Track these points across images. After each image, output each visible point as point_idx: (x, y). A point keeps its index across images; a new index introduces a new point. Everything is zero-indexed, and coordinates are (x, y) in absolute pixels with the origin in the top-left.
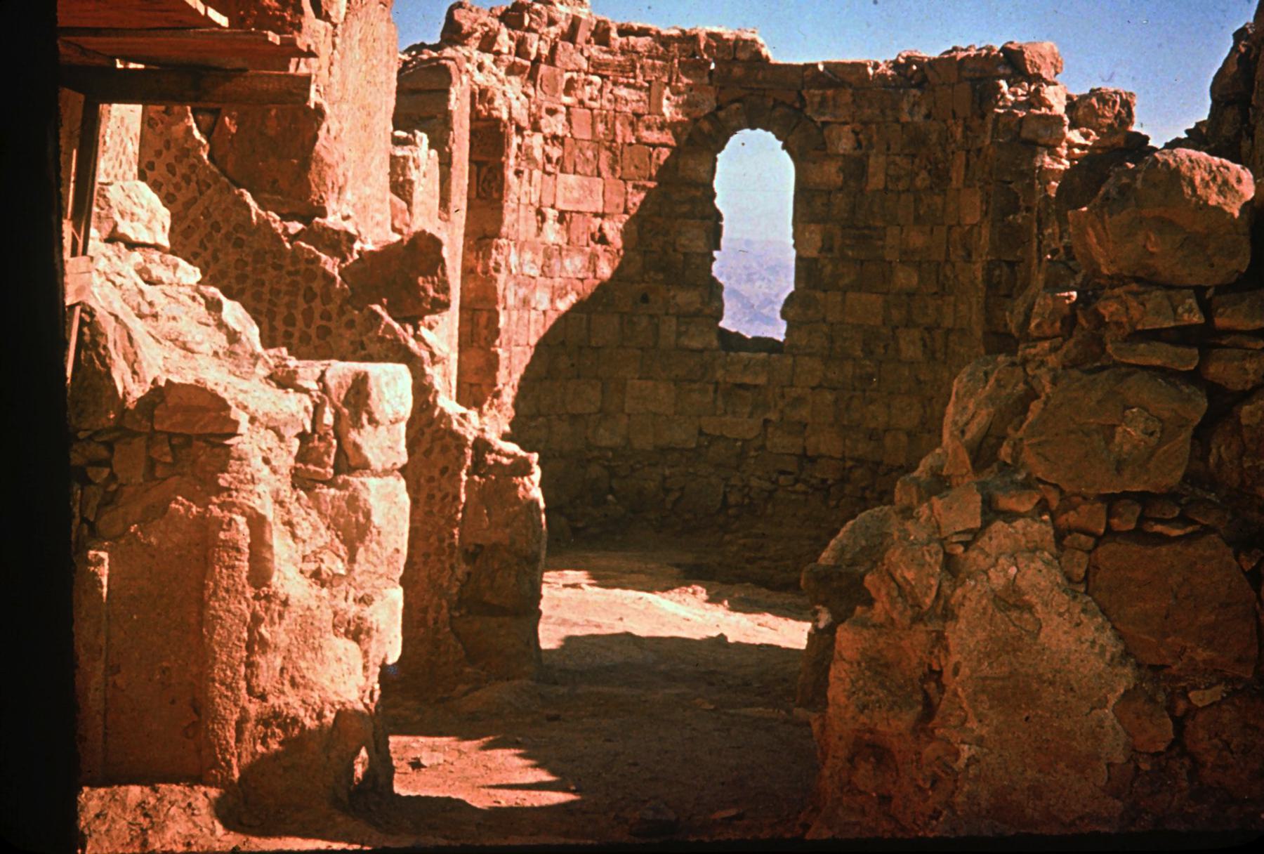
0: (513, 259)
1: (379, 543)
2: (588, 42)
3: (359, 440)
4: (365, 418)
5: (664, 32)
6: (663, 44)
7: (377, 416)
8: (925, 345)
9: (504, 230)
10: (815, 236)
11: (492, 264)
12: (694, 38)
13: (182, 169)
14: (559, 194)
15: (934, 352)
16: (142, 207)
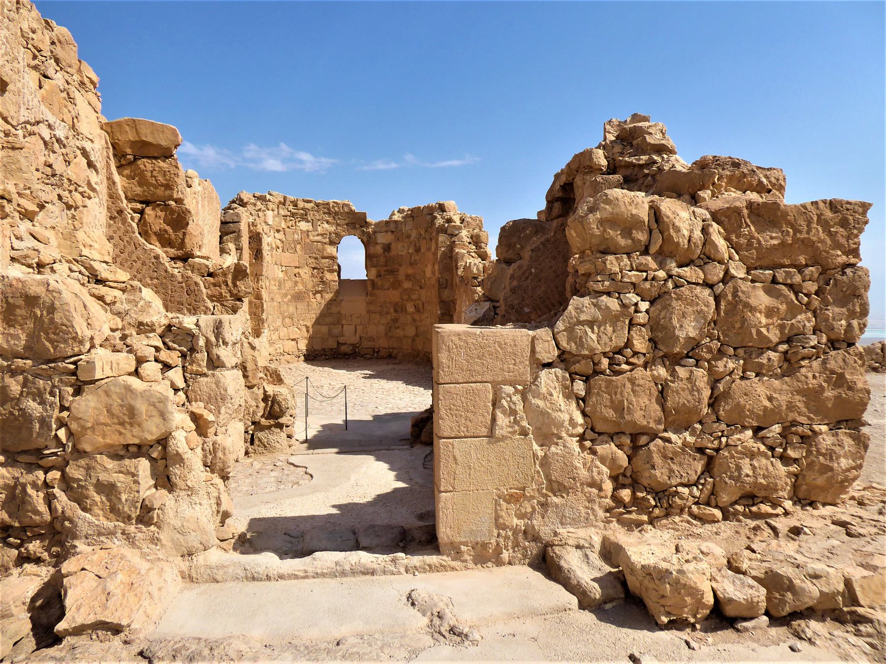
0: (267, 284)
1: (231, 403)
3: (219, 353)
4: (221, 341)
7: (227, 340)
9: (264, 273)
10: (374, 271)
12: (328, 204)
13: (126, 239)
16: (96, 242)
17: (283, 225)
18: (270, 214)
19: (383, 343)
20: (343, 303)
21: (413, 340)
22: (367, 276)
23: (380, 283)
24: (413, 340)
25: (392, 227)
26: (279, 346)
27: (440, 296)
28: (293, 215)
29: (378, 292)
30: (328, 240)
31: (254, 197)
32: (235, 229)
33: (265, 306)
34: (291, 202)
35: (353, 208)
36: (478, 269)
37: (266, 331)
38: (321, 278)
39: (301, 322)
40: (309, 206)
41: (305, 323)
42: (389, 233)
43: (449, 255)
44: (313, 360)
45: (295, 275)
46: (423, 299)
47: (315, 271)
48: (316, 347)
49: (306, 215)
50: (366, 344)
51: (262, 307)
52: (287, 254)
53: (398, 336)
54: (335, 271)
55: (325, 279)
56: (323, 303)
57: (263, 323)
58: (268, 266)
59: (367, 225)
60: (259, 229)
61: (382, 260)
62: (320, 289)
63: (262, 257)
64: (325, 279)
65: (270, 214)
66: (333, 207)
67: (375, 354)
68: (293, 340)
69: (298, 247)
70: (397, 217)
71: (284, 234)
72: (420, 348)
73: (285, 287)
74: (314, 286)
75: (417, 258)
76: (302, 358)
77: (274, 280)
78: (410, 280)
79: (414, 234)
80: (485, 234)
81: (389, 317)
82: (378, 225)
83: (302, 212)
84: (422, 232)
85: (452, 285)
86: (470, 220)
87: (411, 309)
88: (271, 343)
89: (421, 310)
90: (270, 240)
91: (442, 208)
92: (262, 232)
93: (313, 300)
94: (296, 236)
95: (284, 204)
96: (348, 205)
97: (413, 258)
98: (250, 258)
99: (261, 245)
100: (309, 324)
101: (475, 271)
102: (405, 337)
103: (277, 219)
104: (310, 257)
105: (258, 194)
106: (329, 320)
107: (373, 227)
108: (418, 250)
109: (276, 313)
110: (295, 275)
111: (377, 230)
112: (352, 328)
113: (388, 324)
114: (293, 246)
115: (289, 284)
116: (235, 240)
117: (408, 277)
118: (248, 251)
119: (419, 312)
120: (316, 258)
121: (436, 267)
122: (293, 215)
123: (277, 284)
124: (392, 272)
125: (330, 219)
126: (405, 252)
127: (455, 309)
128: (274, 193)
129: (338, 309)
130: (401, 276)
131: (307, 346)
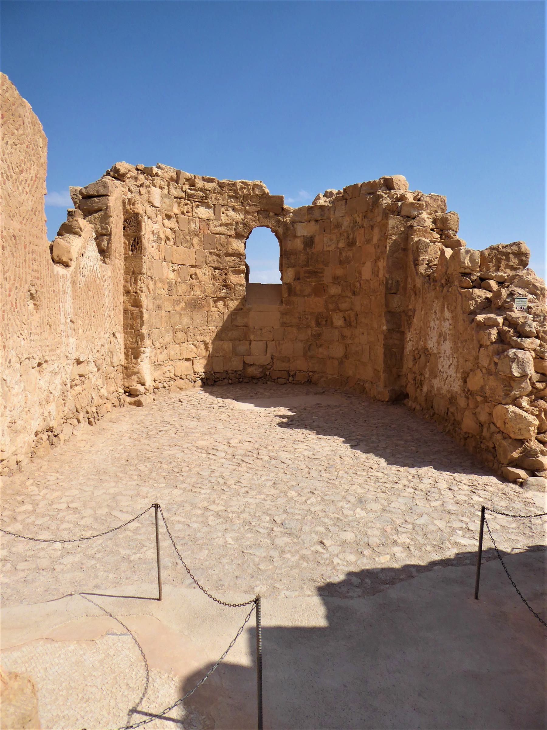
0: (151, 286)
2: (184, 184)
5: (220, 181)
6: (220, 187)
8: (345, 320)
9: (144, 270)
10: (291, 273)
11: (138, 288)
12: (235, 184)
14: (174, 256)
15: (350, 322)
17: (176, 210)
18: (156, 192)
19: (300, 364)
20: (251, 313)
21: (341, 363)
22: (282, 279)
23: (298, 288)
24: (341, 363)
25: (317, 214)
26: (167, 368)
27: (387, 306)
28: (189, 197)
29: (295, 299)
30: (233, 232)
31: (137, 169)
32: (100, 206)
33: (146, 316)
34: (187, 180)
35: (267, 190)
36: (472, 260)
37: (147, 350)
38: (225, 281)
39: (198, 337)
40: (210, 186)
41: (203, 338)
42: (313, 223)
43: (402, 246)
44: (213, 385)
45: (191, 276)
46: (358, 308)
47: (217, 271)
48: (217, 369)
49: (206, 198)
50: (279, 365)
51: (142, 317)
52: (181, 248)
53: (321, 356)
54: (242, 272)
55: (229, 282)
56: (227, 312)
57: (143, 339)
58: (152, 262)
59: (283, 211)
60: (139, 209)
61: (302, 257)
62: (223, 295)
63: (141, 248)
64: (229, 282)
65: (156, 192)
66: (241, 188)
67: (291, 379)
68: (187, 360)
69: (196, 240)
70: (322, 202)
71: (177, 222)
72: (350, 373)
73: (177, 291)
74: (215, 291)
75: (350, 254)
76: (199, 383)
77: (162, 281)
78: (339, 284)
79: (346, 222)
80: (455, 217)
81: (309, 332)
82: (297, 212)
83: (201, 194)
84: (359, 219)
85: (405, 289)
86: (428, 199)
87: (338, 321)
88: (157, 365)
89: (354, 324)
90: (156, 227)
91: (388, 184)
92: (141, 212)
93: (213, 309)
94: (193, 226)
95: (177, 181)
96: (260, 187)
97: (344, 254)
98: (125, 248)
99: (140, 231)
100: (209, 340)
101: (467, 262)
102: (330, 358)
103: (167, 201)
104: (210, 253)
105: (141, 166)
106: (234, 334)
107: (291, 215)
108: (351, 244)
109: (164, 325)
110: (191, 276)
111: (297, 219)
112: (261, 345)
113: (307, 340)
114: (188, 238)
115: (182, 288)
116: (101, 222)
117: (336, 280)
118: (123, 239)
119: (351, 326)
120: (218, 255)
121: (382, 264)
122: (189, 197)
123: (167, 286)
124: (315, 273)
125: (237, 205)
126: (334, 246)
127: (410, 325)
128: (163, 166)
129: (246, 320)
130: (327, 279)
131: (205, 367)
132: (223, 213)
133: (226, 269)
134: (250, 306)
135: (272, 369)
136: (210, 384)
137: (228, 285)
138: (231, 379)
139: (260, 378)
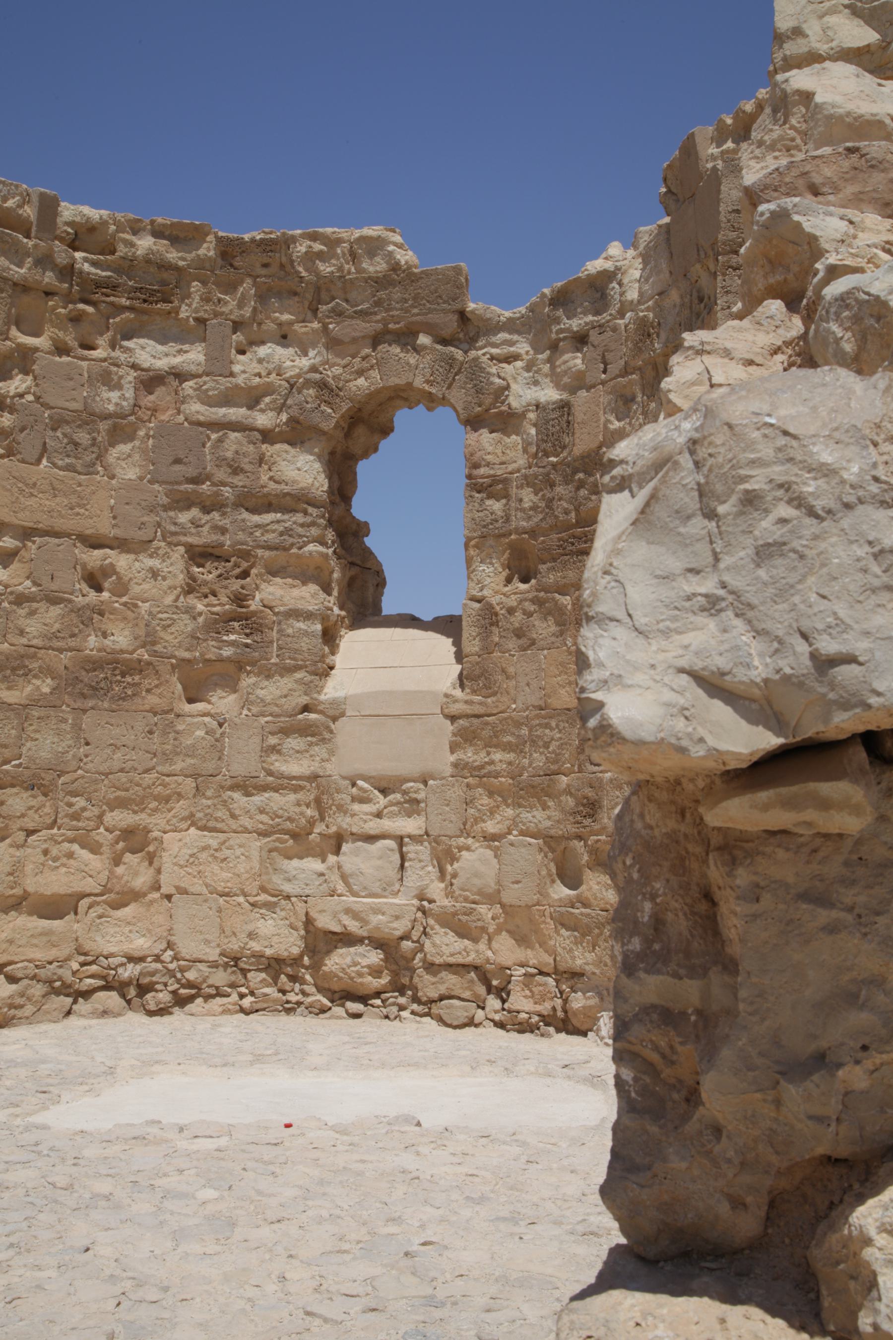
35: (405, 257)
38: (239, 599)
44: (162, 1012)
48: (189, 947)
55: (254, 605)
62: (227, 652)
132: (243, 352)
133: (245, 555)
134: (340, 694)
135: (419, 956)
136: (152, 1007)
137: (254, 613)
138: (252, 993)
139: (378, 994)
